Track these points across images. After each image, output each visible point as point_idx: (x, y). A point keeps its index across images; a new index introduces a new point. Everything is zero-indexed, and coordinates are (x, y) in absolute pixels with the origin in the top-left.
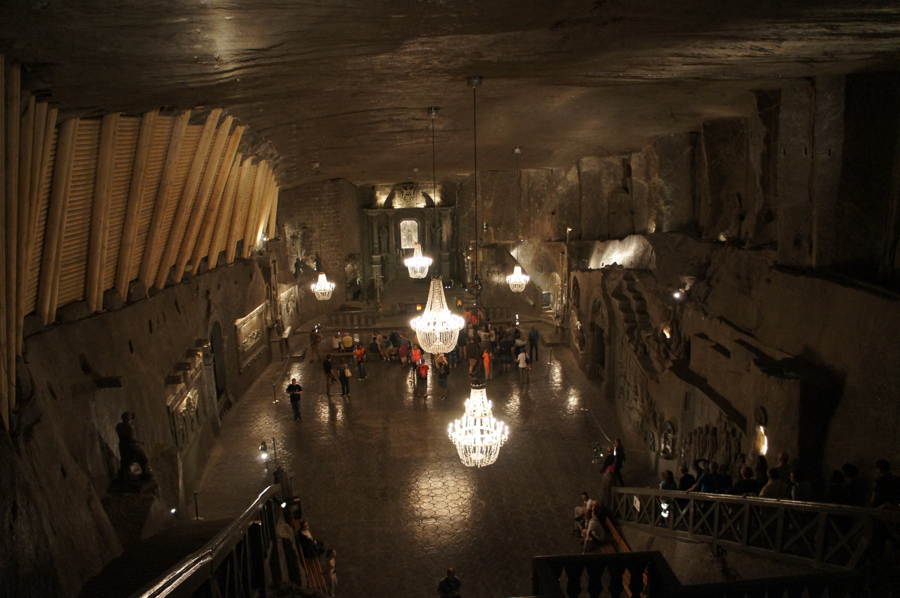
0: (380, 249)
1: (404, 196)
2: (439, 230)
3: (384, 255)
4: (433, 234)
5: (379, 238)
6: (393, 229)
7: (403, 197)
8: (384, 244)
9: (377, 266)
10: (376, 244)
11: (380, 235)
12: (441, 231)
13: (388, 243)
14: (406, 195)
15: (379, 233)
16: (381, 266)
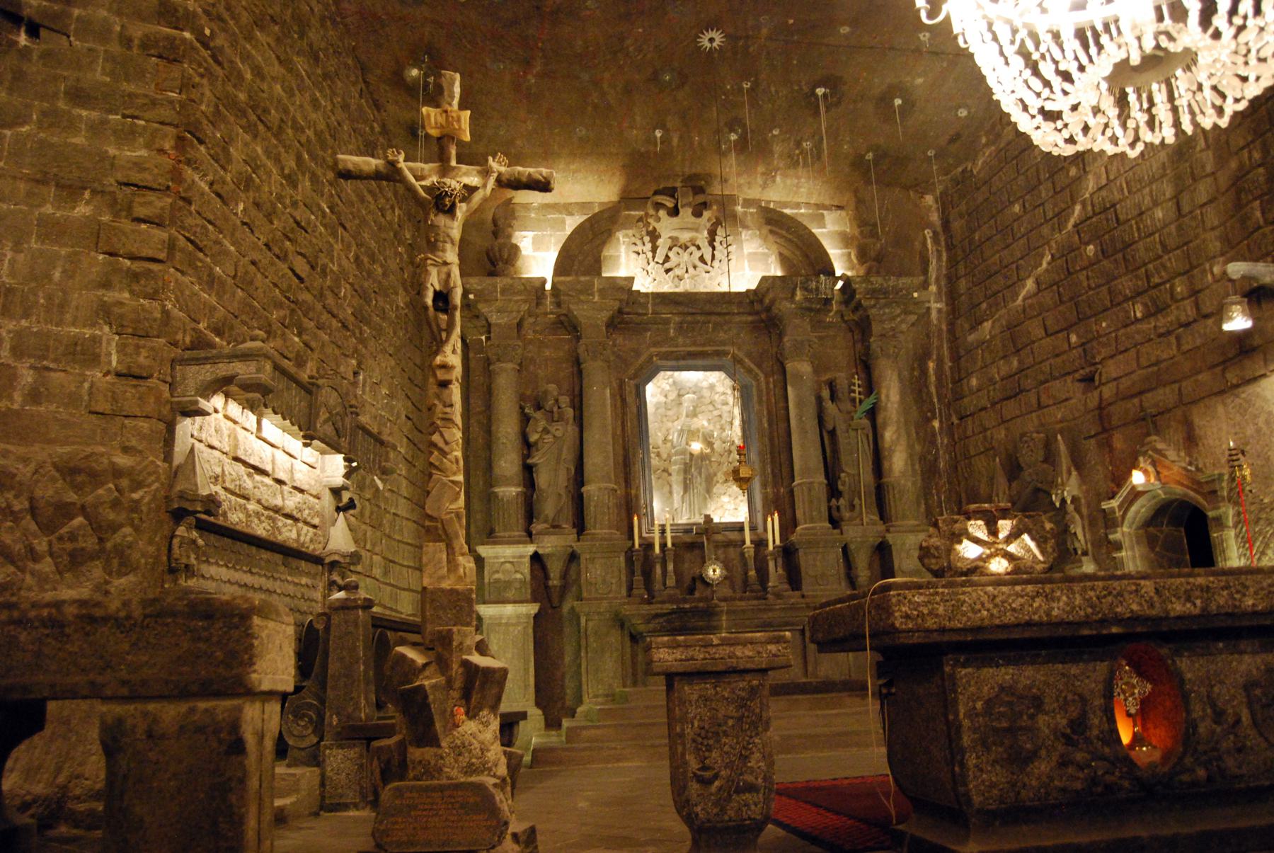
0: (530, 514)
1: (660, 257)
2: (867, 405)
3: (550, 545)
4: (833, 433)
5: (528, 446)
6: (600, 397)
7: (660, 257)
8: (551, 479)
9: (509, 609)
10: (507, 482)
11: (533, 438)
12: (872, 414)
13: (579, 478)
14: (674, 243)
15: (525, 419)
16: (533, 609)
